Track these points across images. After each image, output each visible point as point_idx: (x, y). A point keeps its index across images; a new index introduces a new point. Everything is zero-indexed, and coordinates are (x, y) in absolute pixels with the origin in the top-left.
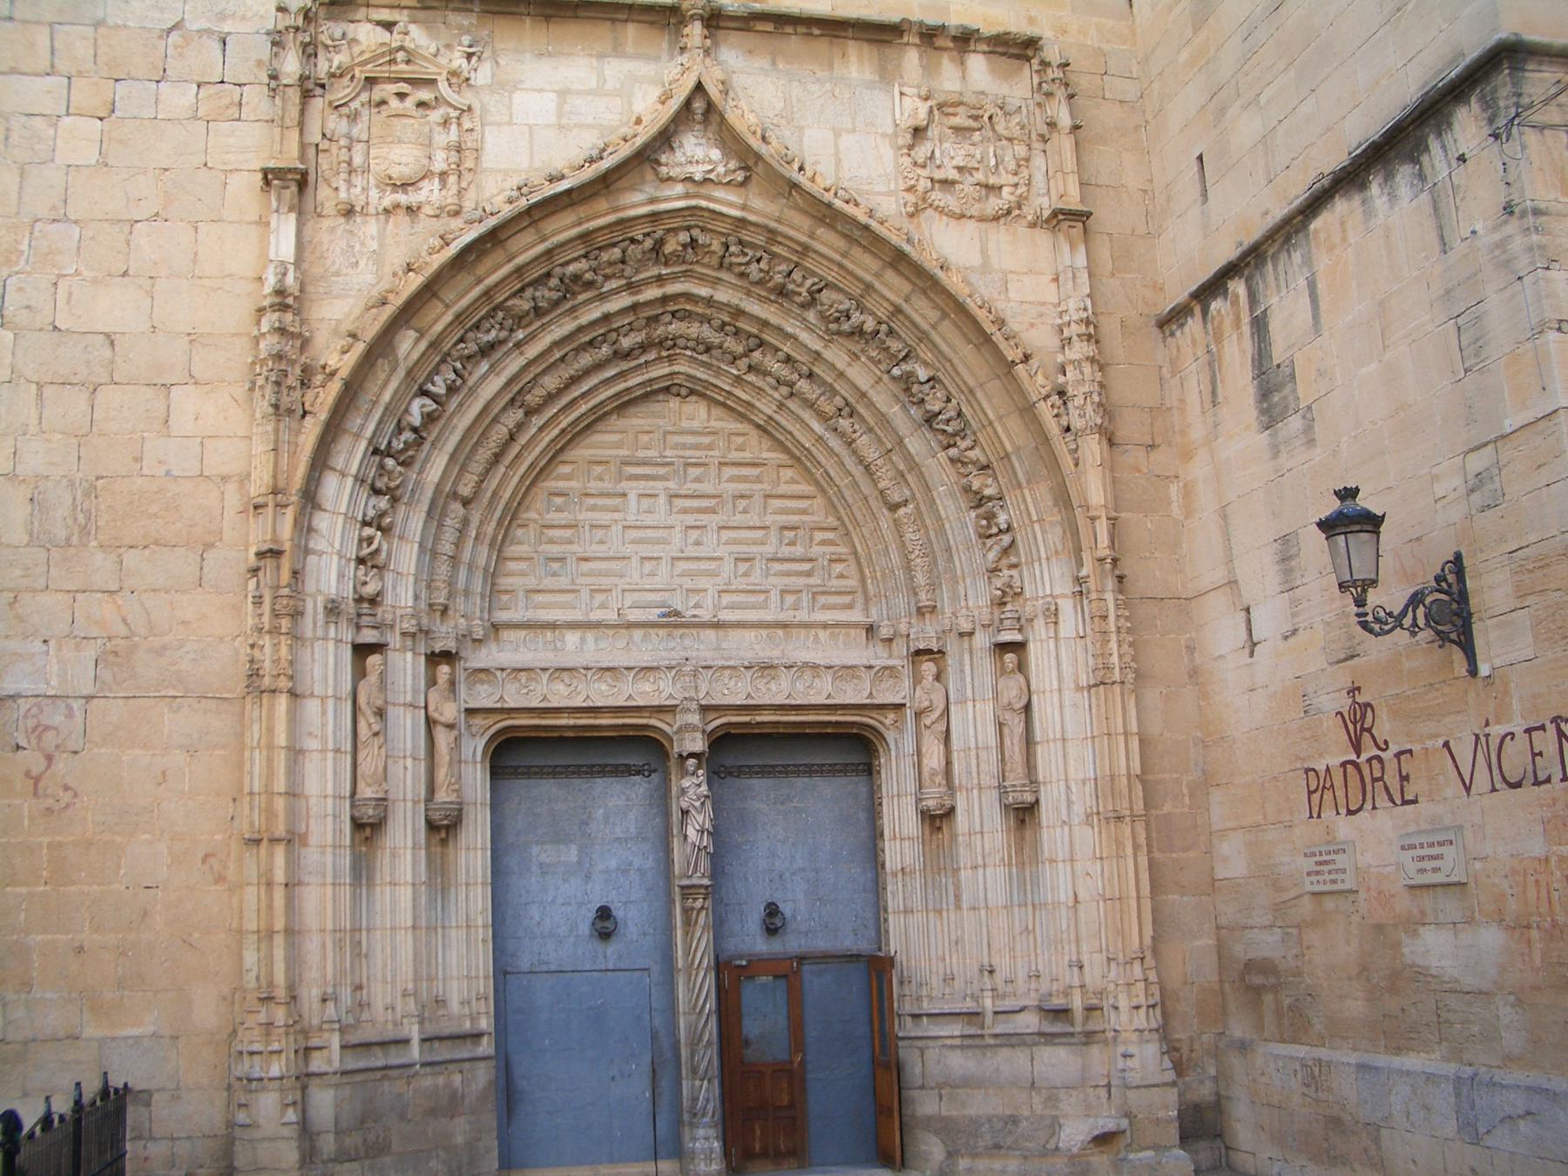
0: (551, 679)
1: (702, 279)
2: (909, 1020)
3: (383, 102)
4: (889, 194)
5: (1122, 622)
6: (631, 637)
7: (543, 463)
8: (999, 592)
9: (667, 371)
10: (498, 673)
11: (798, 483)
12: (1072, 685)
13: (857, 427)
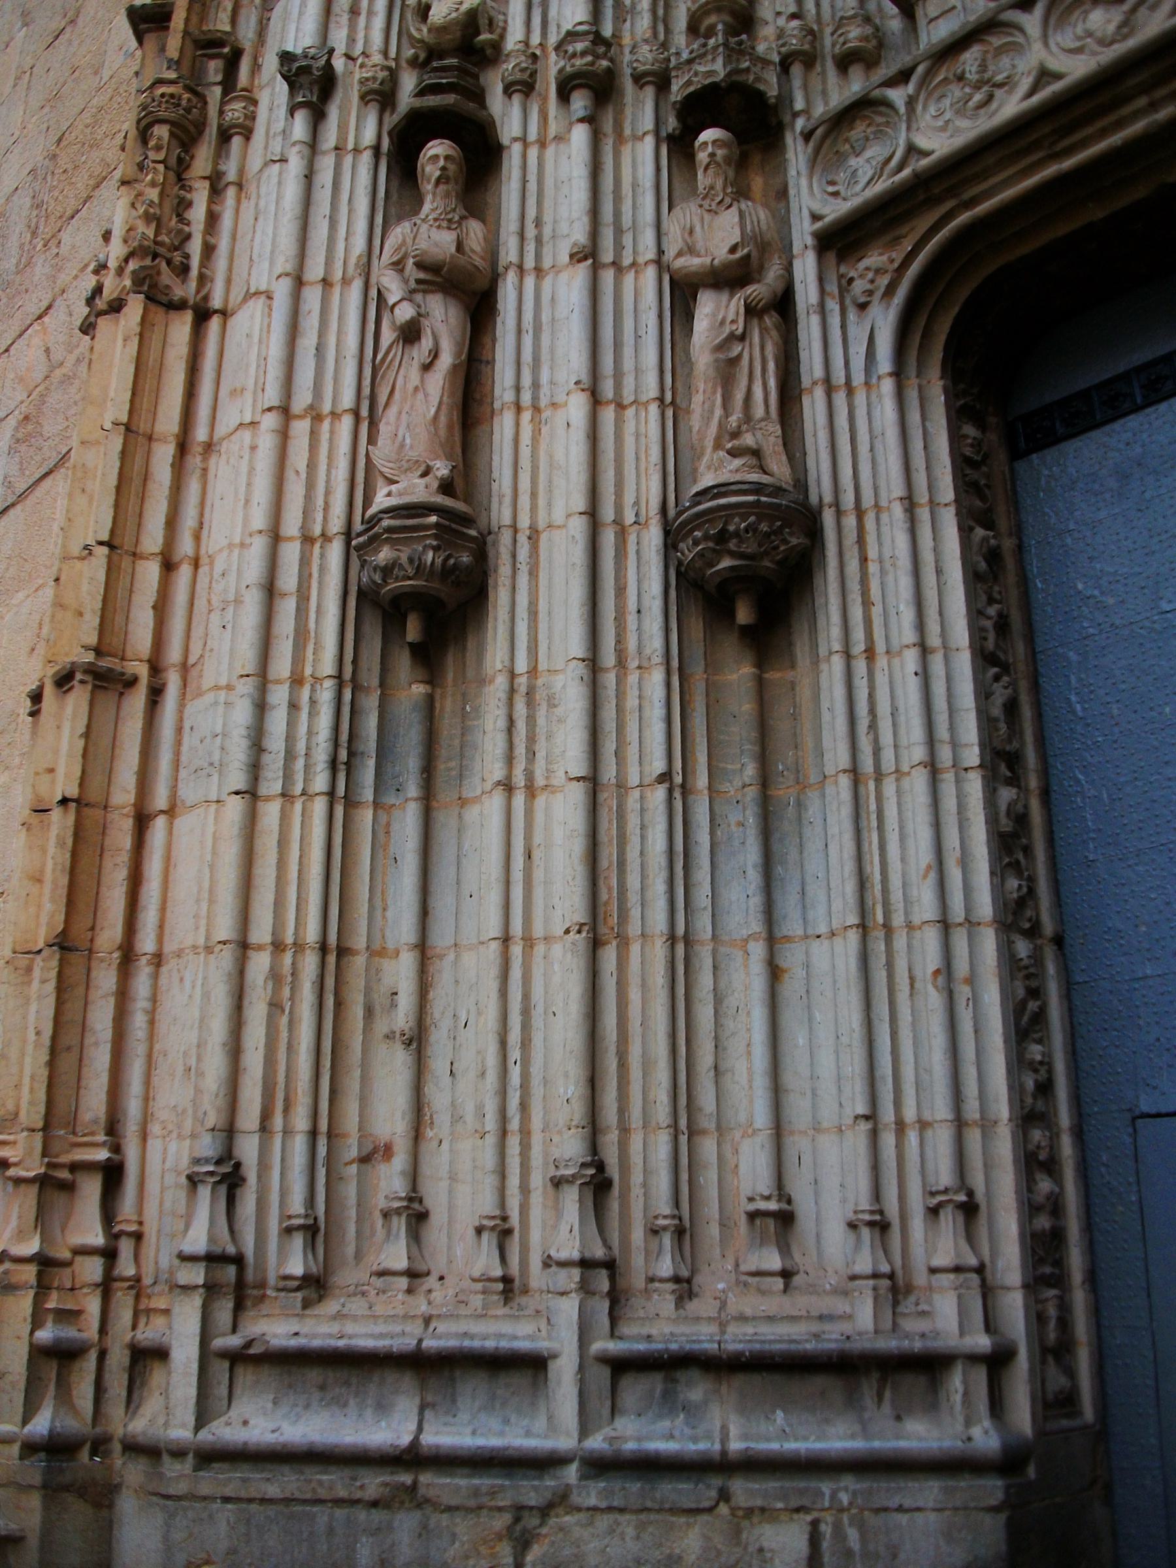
10: (897, 96)
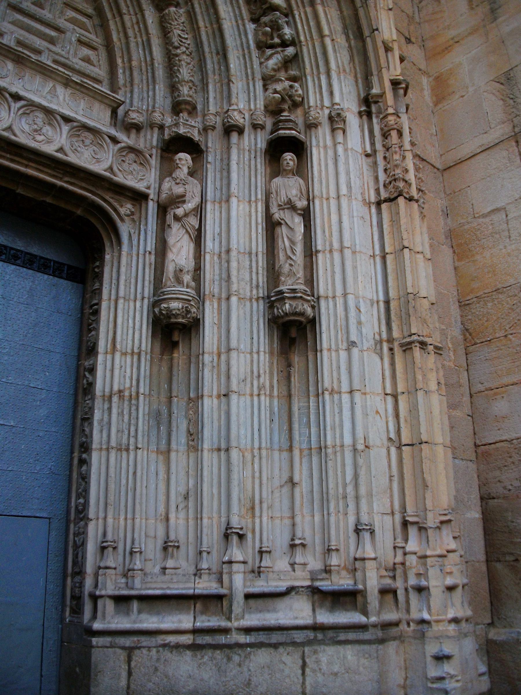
2: (110, 605)
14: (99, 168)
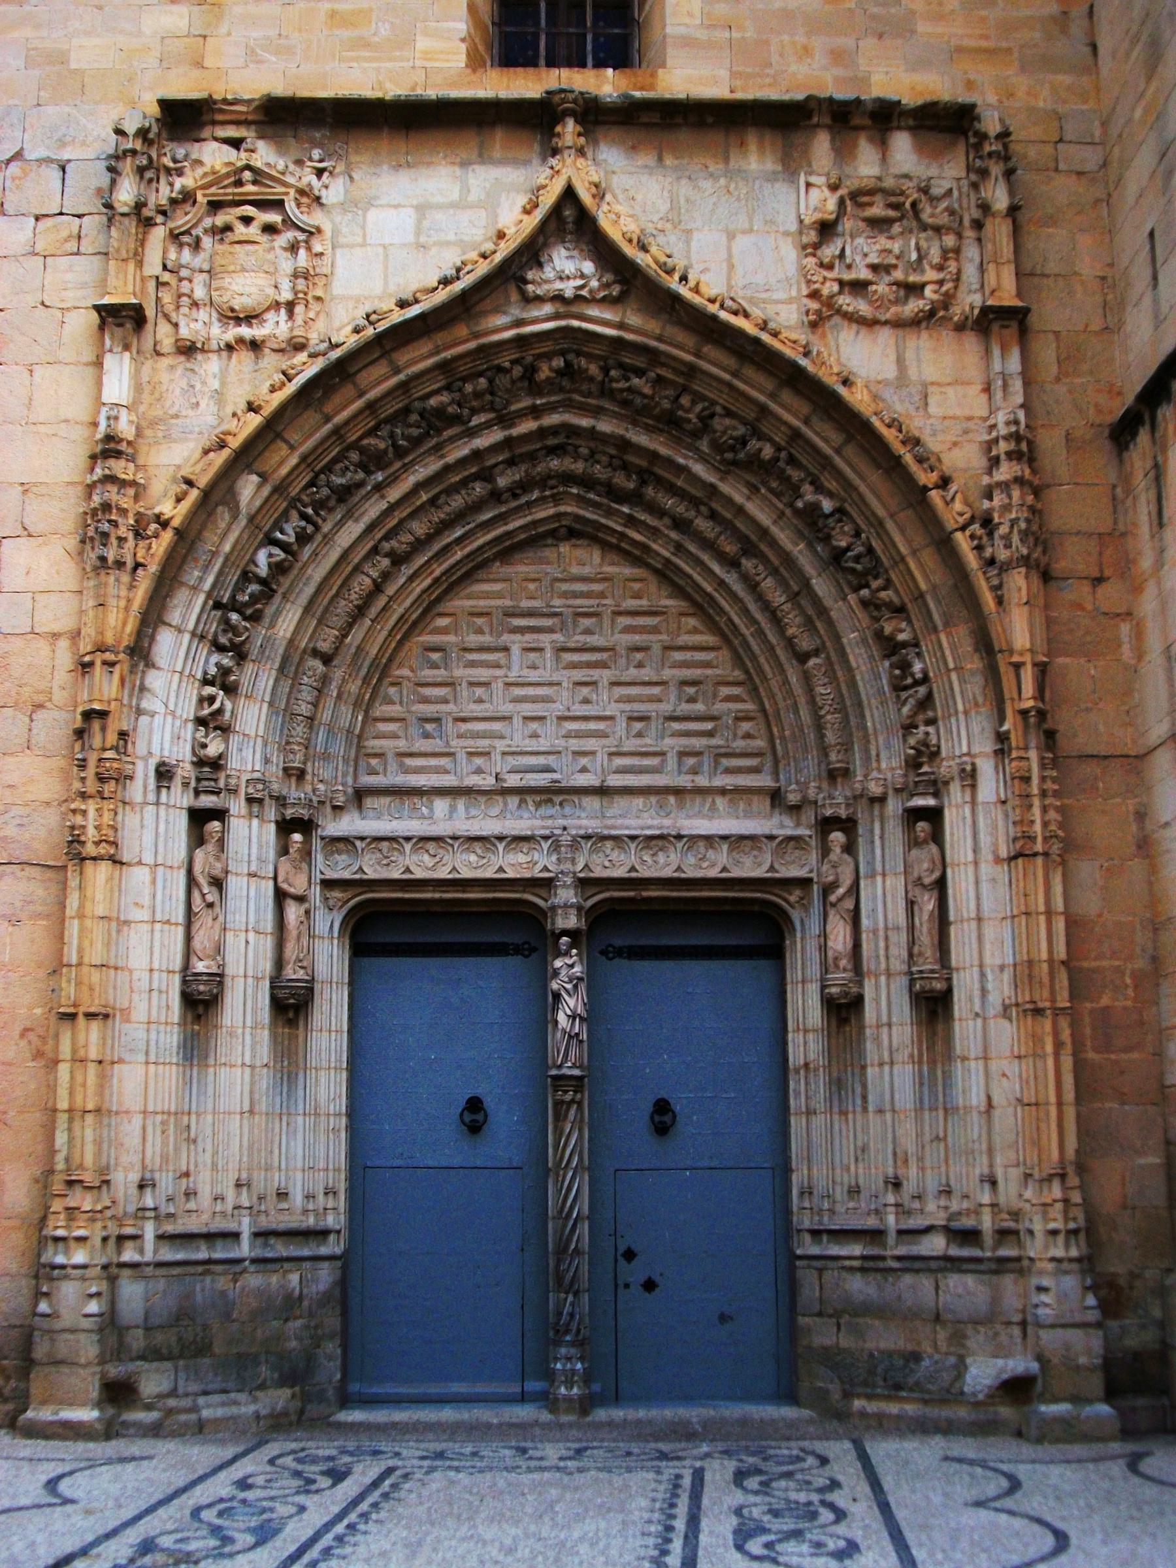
0: (415, 850)
1: (584, 409)
2: (807, 1238)
3: (228, 228)
4: (790, 301)
5: (1050, 786)
6: (506, 804)
7: (414, 616)
8: (912, 752)
9: (551, 511)
10: (358, 843)
11: (701, 633)
12: (990, 857)
13: (761, 567)
14: (760, 873)
